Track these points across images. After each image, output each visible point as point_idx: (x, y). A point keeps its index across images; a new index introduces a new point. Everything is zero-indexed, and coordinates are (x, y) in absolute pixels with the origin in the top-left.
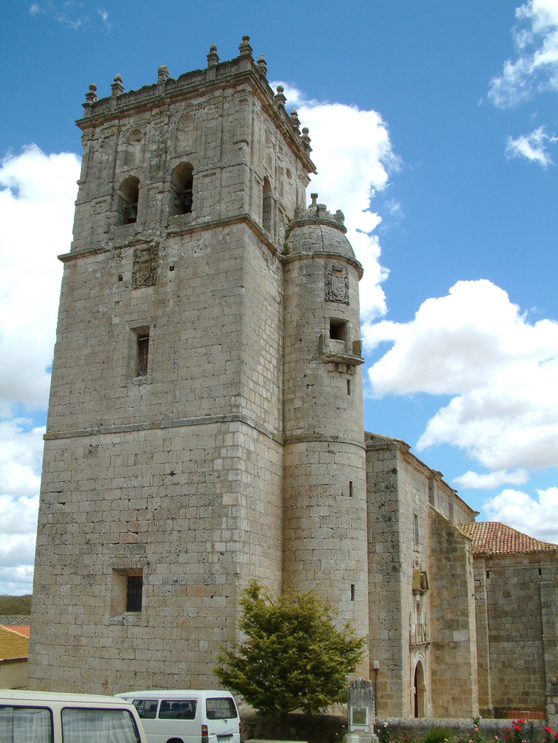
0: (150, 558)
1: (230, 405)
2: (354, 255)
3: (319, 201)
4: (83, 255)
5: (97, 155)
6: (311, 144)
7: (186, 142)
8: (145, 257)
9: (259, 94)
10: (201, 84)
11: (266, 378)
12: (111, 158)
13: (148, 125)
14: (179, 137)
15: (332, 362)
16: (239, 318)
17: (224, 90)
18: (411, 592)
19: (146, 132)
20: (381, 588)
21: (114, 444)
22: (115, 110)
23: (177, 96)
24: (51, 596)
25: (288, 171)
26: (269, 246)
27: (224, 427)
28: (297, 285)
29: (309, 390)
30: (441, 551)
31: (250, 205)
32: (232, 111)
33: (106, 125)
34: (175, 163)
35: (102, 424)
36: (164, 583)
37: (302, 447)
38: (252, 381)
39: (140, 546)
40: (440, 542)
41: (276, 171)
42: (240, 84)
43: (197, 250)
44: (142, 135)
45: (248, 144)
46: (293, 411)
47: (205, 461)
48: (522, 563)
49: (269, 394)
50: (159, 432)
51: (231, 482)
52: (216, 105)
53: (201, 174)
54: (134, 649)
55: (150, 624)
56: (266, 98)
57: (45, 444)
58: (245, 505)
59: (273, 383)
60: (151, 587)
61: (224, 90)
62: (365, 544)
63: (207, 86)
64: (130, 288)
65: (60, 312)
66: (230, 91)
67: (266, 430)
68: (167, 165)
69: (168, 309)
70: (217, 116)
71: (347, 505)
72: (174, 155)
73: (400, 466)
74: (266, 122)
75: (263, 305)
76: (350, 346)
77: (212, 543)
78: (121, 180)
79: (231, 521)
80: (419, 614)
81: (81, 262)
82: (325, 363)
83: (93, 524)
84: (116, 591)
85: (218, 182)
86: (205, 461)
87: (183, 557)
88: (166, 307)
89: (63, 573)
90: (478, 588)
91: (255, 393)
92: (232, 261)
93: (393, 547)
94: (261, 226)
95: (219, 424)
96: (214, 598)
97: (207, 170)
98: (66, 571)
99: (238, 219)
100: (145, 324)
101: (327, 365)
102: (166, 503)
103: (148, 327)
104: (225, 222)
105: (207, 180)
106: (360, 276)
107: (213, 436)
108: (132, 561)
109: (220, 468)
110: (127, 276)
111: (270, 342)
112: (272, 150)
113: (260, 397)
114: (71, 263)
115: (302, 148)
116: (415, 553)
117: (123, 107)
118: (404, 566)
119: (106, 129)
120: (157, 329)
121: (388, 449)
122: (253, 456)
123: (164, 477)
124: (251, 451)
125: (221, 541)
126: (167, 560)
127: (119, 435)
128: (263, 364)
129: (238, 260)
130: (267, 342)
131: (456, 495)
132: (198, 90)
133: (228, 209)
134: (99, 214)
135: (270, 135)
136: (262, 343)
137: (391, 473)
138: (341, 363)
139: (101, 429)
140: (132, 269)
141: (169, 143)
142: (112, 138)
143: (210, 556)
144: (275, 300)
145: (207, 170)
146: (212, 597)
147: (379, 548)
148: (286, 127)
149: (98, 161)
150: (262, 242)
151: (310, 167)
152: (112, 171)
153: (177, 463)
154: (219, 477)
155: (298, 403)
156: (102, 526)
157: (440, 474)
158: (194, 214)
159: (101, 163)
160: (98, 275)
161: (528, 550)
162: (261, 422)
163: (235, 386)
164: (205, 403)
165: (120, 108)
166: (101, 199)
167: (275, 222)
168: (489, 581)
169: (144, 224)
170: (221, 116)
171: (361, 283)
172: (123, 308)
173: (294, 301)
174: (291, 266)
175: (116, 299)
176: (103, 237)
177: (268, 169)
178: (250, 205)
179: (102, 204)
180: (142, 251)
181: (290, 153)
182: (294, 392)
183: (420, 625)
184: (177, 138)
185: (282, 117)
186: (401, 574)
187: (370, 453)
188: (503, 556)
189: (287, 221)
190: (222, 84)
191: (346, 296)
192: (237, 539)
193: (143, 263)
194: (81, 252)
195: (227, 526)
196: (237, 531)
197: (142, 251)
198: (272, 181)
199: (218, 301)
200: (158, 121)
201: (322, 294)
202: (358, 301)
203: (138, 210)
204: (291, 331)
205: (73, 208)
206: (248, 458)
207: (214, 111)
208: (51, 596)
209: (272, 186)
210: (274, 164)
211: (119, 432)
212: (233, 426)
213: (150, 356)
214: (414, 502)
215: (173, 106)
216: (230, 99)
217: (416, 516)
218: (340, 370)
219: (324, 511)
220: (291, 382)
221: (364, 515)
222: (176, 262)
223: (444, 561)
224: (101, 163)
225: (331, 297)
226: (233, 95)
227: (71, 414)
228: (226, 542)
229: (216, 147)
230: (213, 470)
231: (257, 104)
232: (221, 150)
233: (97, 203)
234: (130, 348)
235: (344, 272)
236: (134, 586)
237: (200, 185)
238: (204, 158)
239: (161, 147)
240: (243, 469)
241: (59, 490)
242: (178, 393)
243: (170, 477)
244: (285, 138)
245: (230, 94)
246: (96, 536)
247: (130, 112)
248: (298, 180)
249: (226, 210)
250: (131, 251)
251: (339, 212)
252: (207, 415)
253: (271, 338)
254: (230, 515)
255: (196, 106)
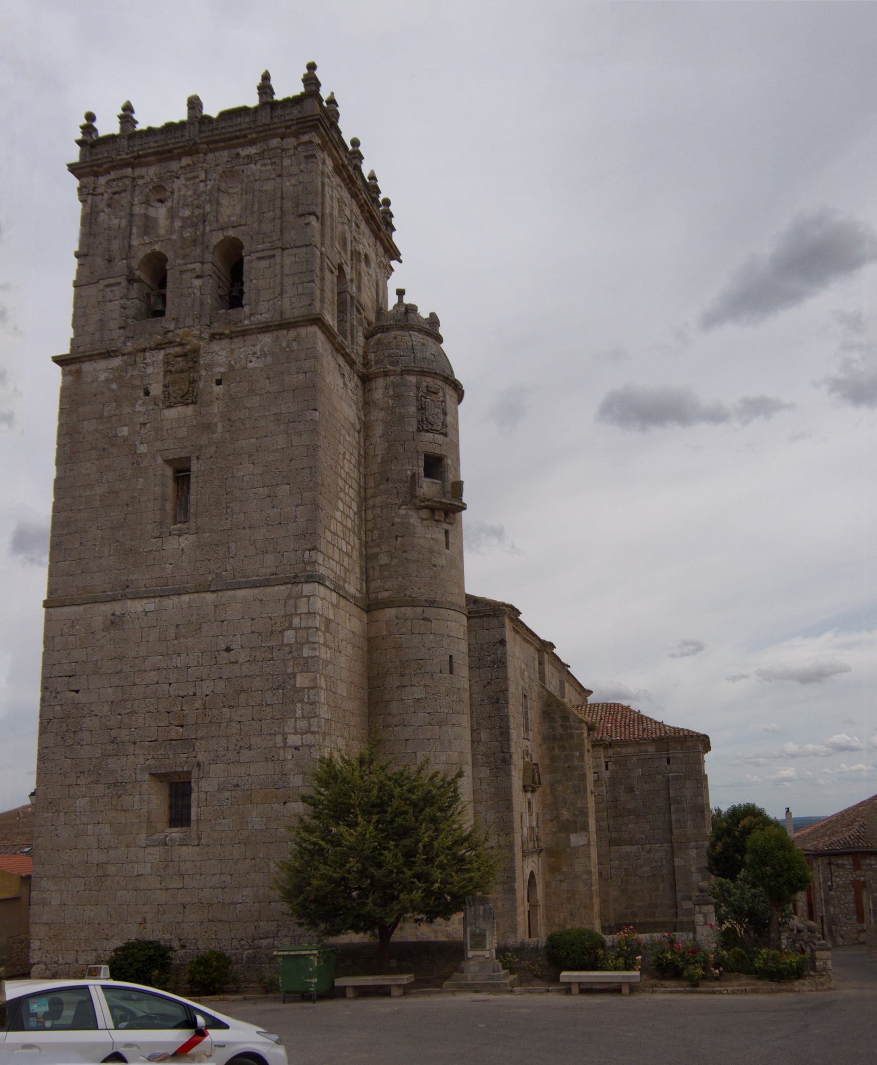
0: (200, 758)
1: (304, 562)
2: (452, 372)
3: (407, 300)
4: (91, 358)
5: (103, 217)
6: (395, 222)
7: (230, 208)
8: (181, 363)
9: (330, 150)
10: (250, 128)
11: (346, 527)
12: (124, 223)
13: (175, 180)
14: (221, 200)
15: (426, 507)
16: (312, 450)
17: (282, 139)
18: (521, 788)
19: (173, 190)
20: (489, 784)
21: (146, 613)
22: (127, 154)
23: (217, 142)
24: (62, 814)
25: (366, 256)
26: (346, 356)
27: (296, 589)
28: (382, 409)
29: (398, 542)
30: (555, 738)
31: (322, 301)
32: (295, 170)
33: (113, 175)
34: (217, 238)
35: (128, 587)
36: (220, 790)
37: (391, 612)
38: (330, 530)
39: (187, 743)
40: (553, 728)
41: (352, 256)
42: (305, 133)
43: (254, 359)
44: (168, 194)
45: (317, 218)
46: (378, 568)
47: (272, 633)
48: (647, 751)
49: (349, 547)
50: (210, 597)
51: (307, 658)
52: (273, 160)
53: (254, 256)
54: (182, 875)
55: (203, 842)
56: (340, 155)
57: (47, 613)
58: (324, 687)
59: (354, 533)
60: (203, 796)
61: (282, 139)
62: (468, 731)
63: (259, 132)
64: (161, 405)
65: (60, 435)
66: (291, 142)
67: (346, 592)
68: (206, 239)
69: (215, 436)
70: (273, 176)
71: (447, 685)
72: (215, 226)
73: (509, 635)
74: (339, 189)
75: (341, 434)
76: (449, 487)
77: (283, 735)
78: (141, 255)
79: (307, 708)
80: (531, 815)
81: (87, 367)
82: (418, 509)
83: (120, 717)
84: (156, 801)
85: (278, 267)
86: (272, 633)
87: (245, 755)
88: (214, 433)
89: (79, 782)
90: (597, 782)
91: (334, 545)
92: (301, 376)
93: (502, 734)
94: (336, 330)
95: (289, 586)
96: (288, 805)
97: (263, 250)
98: (83, 780)
99: (308, 320)
100: (183, 455)
101: (420, 512)
102: (221, 686)
103: (188, 459)
104: (289, 323)
105: (264, 264)
106: (460, 398)
107: (282, 602)
108: (178, 761)
109: (293, 641)
110: (156, 390)
111: (349, 481)
112: (346, 227)
113: (338, 553)
114: (73, 367)
115: (383, 227)
116: (525, 743)
117: (138, 151)
118: (515, 757)
119: (114, 180)
120: (200, 461)
121: (495, 616)
122: (333, 626)
123: (217, 653)
124: (330, 620)
125: (295, 733)
126: (224, 759)
127: (153, 600)
128: (342, 509)
129: (309, 375)
130: (346, 482)
131: (568, 671)
132: (245, 136)
133: (294, 305)
134: (110, 301)
135: (344, 206)
136: (341, 483)
137: (498, 645)
138: (438, 509)
139: (127, 592)
140: (162, 380)
141: (208, 208)
142: (123, 195)
143: (281, 752)
144: (354, 428)
145: (263, 250)
146: (285, 803)
147: (484, 736)
148: (364, 196)
149: (106, 226)
150: (337, 350)
151: (393, 253)
152: (126, 242)
153: (234, 636)
154: (290, 652)
155: (384, 559)
156: (133, 718)
157: (552, 646)
158: (246, 309)
159: (109, 229)
160: (114, 386)
161: (654, 736)
162: (341, 583)
163: (309, 537)
164: (270, 559)
165: (133, 152)
166: (112, 281)
167: (352, 325)
168: (608, 773)
169: (176, 320)
170: (280, 176)
171: (461, 408)
172: (153, 433)
173: (379, 430)
174: (373, 384)
175: (141, 420)
176: (116, 333)
177: (343, 254)
178: (322, 301)
179: (115, 288)
180: (176, 357)
181: (367, 232)
182: (379, 545)
183: (531, 828)
184: (218, 203)
185: (359, 183)
186: (512, 766)
187: (473, 621)
188: (624, 743)
189: (366, 325)
190: (279, 131)
191: (444, 425)
192: (316, 730)
193: (177, 372)
194: (87, 354)
195: (303, 714)
196: (316, 720)
197: (176, 357)
198: (347, 269)
199: (283, 427)
200: (189, 175)
201: (414, 422)
202: (457, 431)
203: (168, 299)
204: (375, 468)
205: (71, 291)
206: (327, 630)
207: (269, 167)
208: (62, 814)
209: (348, 277)
210: (349, 248)
211: (154, 597)
212: (307, 588)
213: (192, 498)
214: (523, 679)
215: (210, 156)
216: (292, 152)
217: (525, 696)
218: (437, 518)
219: (419, 693)
220: (376, 532)
221: (466, 696)
222: (224, 373)
223: (557, 752)
224: (109, 229)
225: (424, 425)
226: (296, 148)
227: (83, 572)
228: (302, 734)
229: (274, 219)
230: (283, 644)
231: (327, 162)
232: (282, 223)
233: (107, 286)
234: (164, 485)
235: (440, 394)
236: (179, 793)
237: (253, 271)
238: (258, 233)
239: (196, 213)
240: (322, 642)
241: (69, 674)
242: (233, 545)
243: (225, 654)
244: (362, 212)
245: (291, 146)
246: (125, 732)
247: (148, 159)
248: (378, 270)
249: (291, 307)
250: (160, 355)
251: (433, 316)
252: (273, 574)
253: (350, 477)
254: (306, 700)
255: (244, 158)
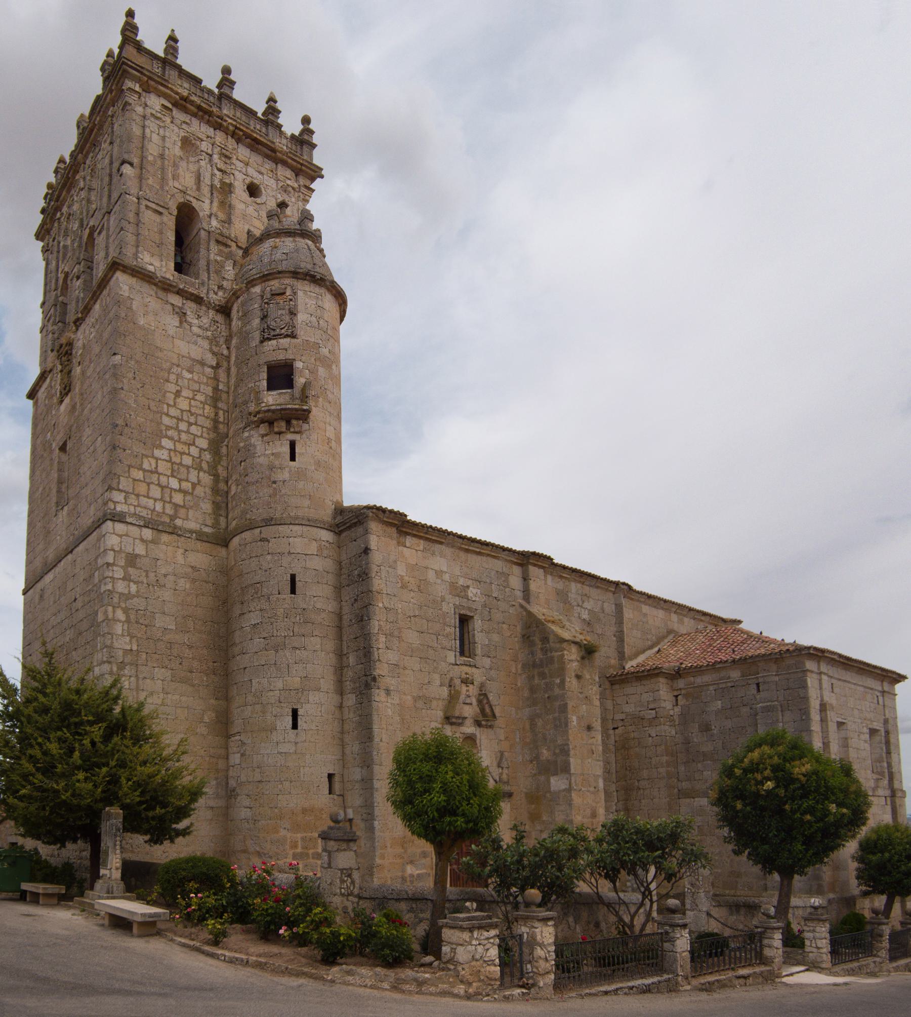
71: (286, 606)
218: (276, 430)
